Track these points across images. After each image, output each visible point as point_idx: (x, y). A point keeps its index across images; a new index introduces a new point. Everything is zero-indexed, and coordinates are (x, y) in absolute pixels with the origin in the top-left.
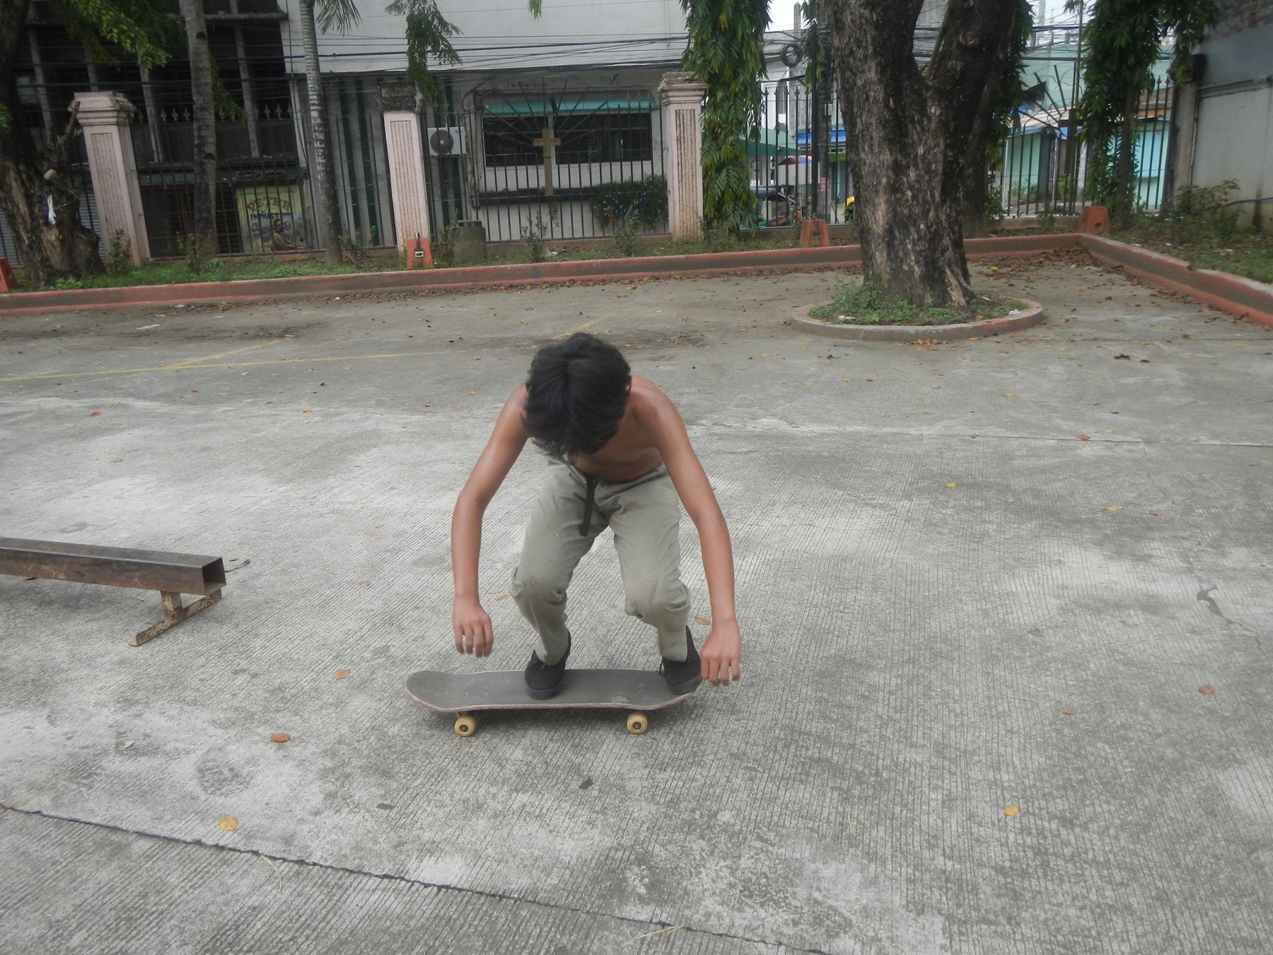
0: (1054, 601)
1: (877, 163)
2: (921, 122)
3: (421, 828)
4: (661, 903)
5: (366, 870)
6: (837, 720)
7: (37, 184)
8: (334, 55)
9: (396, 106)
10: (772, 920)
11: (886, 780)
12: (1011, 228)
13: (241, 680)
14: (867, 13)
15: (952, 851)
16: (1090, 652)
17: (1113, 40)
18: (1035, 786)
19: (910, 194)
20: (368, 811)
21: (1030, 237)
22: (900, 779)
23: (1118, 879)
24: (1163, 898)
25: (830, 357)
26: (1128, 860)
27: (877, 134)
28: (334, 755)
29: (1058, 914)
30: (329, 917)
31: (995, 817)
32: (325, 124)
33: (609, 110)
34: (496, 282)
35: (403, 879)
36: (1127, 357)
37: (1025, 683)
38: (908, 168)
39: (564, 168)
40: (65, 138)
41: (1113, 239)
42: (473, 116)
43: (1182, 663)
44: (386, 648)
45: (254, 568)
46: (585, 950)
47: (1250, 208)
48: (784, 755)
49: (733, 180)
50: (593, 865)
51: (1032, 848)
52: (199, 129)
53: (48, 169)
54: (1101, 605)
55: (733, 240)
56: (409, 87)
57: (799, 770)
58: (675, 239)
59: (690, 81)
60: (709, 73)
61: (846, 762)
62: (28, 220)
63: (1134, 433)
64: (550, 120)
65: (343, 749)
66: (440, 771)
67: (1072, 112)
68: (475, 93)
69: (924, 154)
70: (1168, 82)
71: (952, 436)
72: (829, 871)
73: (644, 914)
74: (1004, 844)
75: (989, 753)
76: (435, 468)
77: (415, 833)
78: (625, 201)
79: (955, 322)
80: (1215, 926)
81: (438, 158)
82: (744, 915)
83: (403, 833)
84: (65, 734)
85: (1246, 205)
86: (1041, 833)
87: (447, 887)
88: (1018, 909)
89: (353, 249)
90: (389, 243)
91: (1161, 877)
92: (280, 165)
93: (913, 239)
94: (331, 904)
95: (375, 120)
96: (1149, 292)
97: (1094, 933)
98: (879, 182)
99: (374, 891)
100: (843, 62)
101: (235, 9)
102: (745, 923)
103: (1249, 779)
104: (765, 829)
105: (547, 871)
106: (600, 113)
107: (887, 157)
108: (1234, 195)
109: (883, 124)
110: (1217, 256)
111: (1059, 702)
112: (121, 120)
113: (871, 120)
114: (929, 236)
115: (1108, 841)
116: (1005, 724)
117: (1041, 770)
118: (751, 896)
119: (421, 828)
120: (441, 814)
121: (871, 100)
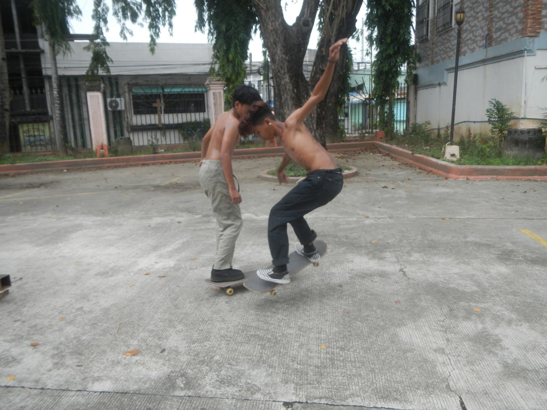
0: (348, 275)
3: (94, 372)
4: (189, 389)
5: (70, 389)
6: (263, 321)
8: (65, 68)
10: (231, 391)
11: (279, 340)
12: (349, 139)
13: (17, 324)
14: (284, 56)
15: (300, 362)
16: (359, 292)
17: (383, 68)
18: (333, 338)
20: (72, 368)
21: (355, 143)
22: (284, 339)
23: (358, 366)
24: (373, 371)
25: (274, 190)
26: (362, 359)
27: (290, 103)
28: (58, 348)
29: (335, 379)
30: (54, 407)
31: (317, 349)
33: (185, 92)
34: (138, 163)
35: (85, 391)
36: (387, 187)
37: (334, 303)
39: (166, 115)
41: (387, 143)
42: (127, 95)
43: (390, 293)
44: (82, 308)
45: (24, 280)
46: (158, 408)
47: (436, 131)
48: (242, 335)
50: (163, 379)
51: (329, 358)
54: (365, 275)
56: (98, 82)
57: (247, 339)
59: (219, 80)
60: (226, 78)
61: (265, 335)
63: (386, 215)
65: (62, 347)
66: (103, 351)
67: (370, 95)
68: (128, 84)
70: (404, 84)
71: (318, 218)
72: (254, 373)
73: (182, 394)
74: (319, 358)
75: (318, 328)
76: (107, 238)
77: (91, 374)
78: (194, 129)
80: (389, 378)
82: (221, 390)
83: (86, 375)
85: (435, 130)
86: (333, 353)
87: (104, 392)
88: (322, 379)
89: (72, 149)
90: (89, 146)
91: (372, 364)
92: (40, 114)
94: (55, 402)
95: (83, 95)
96: (398, 163)
97: (347, 384)
99: (73, 396)
102: (221, 393)
103: (407, 330)
104: (232, 361)
105: (145, 383)
106: (180, 93)
108: (429, 127)
109: (292, 98)
110: (423, 150)
111: (345, 309)
115: (356, 354)
116: (325, 318)
117: (336, 332)
118: (224, 384)
119: (94, 372)
120: (102, 366)
121: (287, 89)
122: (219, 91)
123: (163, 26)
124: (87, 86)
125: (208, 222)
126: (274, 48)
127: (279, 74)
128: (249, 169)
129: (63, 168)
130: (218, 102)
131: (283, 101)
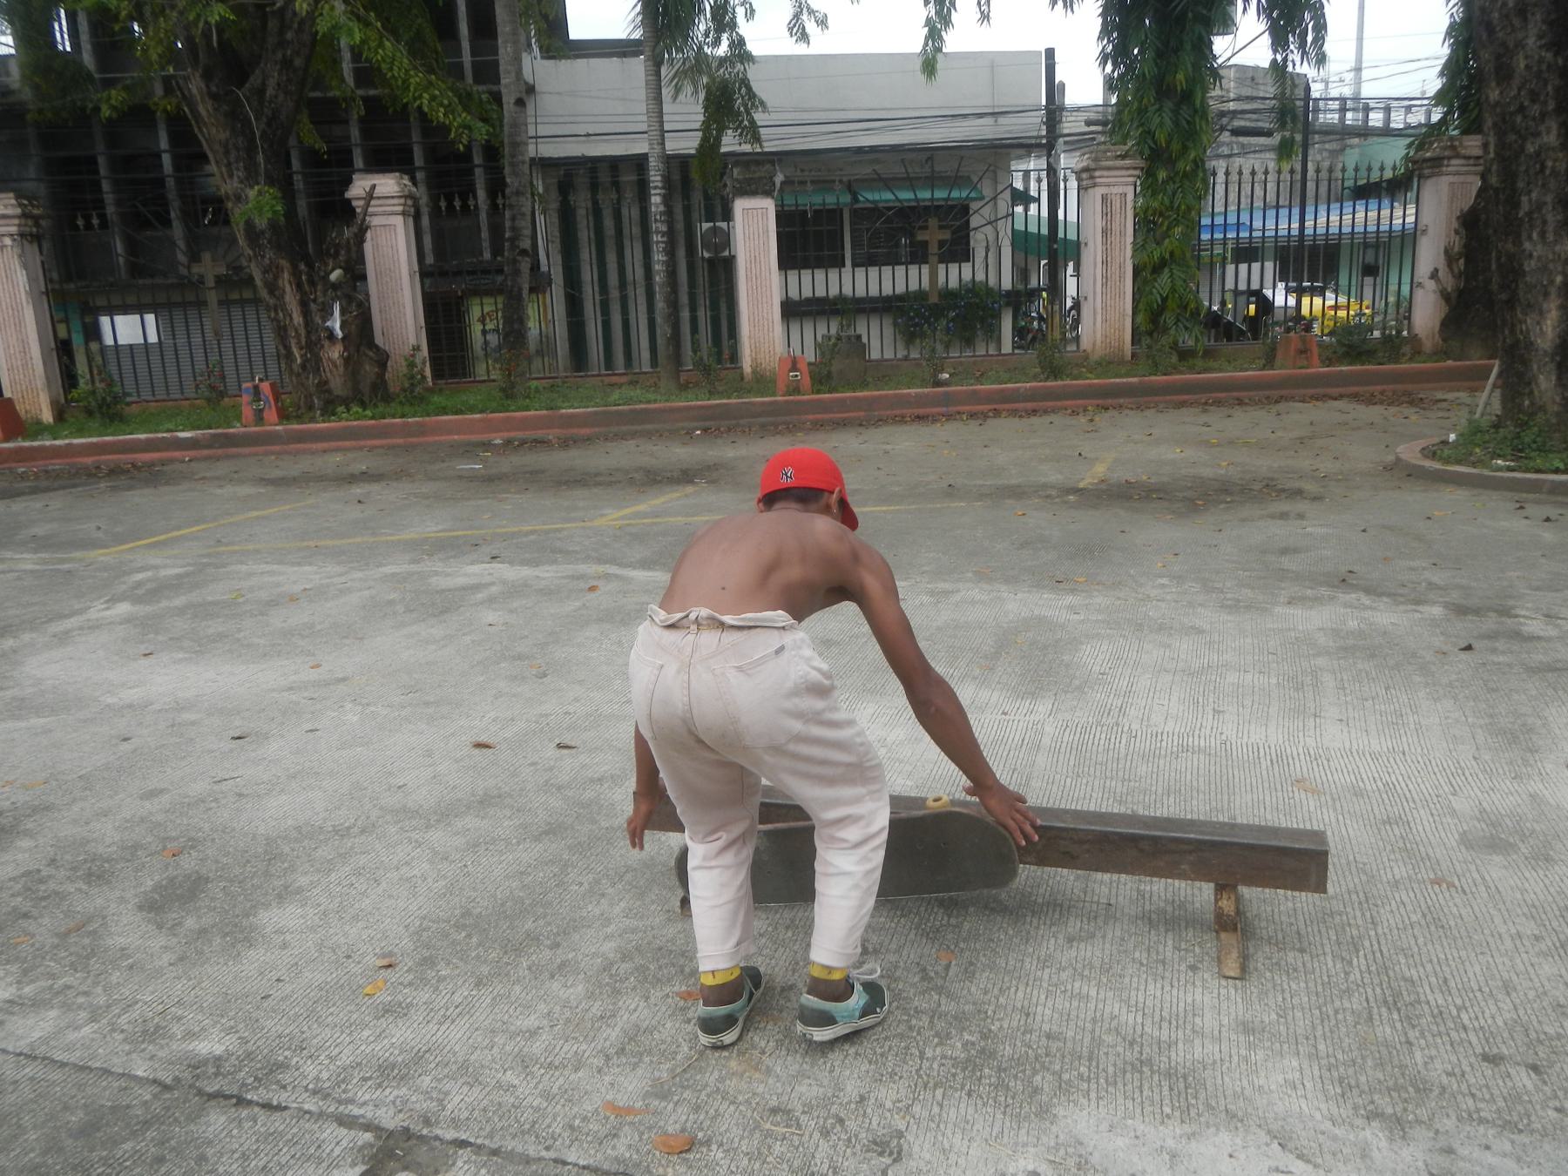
1: (1551, 257)
7: (319, 287)
8: (588, 135)
9: (751, 188)
14: (1549, 56)
25: (1548, 520)
32: (669, 212)
34: (898, 412)
39: (860, 272)
40: (355, 229)
49: (1179, 283)
52: (513, 219)
55: (1174, 359)
56: (768, 166)
58: (1095, 357)
59: (1123, 157)
60: (1150, 147)
62: (303, 332)
76: (1232, 678)
78: (937, 312)
81: (710, 261)
98: (1552, 282)
100: (1504, 119)
101: (469, 79)
121: (1548, 172)
122: (1119, 190)
124: (737, 180)
128: (1301, 440)
129: (686, 424)
130: (1116, 227)
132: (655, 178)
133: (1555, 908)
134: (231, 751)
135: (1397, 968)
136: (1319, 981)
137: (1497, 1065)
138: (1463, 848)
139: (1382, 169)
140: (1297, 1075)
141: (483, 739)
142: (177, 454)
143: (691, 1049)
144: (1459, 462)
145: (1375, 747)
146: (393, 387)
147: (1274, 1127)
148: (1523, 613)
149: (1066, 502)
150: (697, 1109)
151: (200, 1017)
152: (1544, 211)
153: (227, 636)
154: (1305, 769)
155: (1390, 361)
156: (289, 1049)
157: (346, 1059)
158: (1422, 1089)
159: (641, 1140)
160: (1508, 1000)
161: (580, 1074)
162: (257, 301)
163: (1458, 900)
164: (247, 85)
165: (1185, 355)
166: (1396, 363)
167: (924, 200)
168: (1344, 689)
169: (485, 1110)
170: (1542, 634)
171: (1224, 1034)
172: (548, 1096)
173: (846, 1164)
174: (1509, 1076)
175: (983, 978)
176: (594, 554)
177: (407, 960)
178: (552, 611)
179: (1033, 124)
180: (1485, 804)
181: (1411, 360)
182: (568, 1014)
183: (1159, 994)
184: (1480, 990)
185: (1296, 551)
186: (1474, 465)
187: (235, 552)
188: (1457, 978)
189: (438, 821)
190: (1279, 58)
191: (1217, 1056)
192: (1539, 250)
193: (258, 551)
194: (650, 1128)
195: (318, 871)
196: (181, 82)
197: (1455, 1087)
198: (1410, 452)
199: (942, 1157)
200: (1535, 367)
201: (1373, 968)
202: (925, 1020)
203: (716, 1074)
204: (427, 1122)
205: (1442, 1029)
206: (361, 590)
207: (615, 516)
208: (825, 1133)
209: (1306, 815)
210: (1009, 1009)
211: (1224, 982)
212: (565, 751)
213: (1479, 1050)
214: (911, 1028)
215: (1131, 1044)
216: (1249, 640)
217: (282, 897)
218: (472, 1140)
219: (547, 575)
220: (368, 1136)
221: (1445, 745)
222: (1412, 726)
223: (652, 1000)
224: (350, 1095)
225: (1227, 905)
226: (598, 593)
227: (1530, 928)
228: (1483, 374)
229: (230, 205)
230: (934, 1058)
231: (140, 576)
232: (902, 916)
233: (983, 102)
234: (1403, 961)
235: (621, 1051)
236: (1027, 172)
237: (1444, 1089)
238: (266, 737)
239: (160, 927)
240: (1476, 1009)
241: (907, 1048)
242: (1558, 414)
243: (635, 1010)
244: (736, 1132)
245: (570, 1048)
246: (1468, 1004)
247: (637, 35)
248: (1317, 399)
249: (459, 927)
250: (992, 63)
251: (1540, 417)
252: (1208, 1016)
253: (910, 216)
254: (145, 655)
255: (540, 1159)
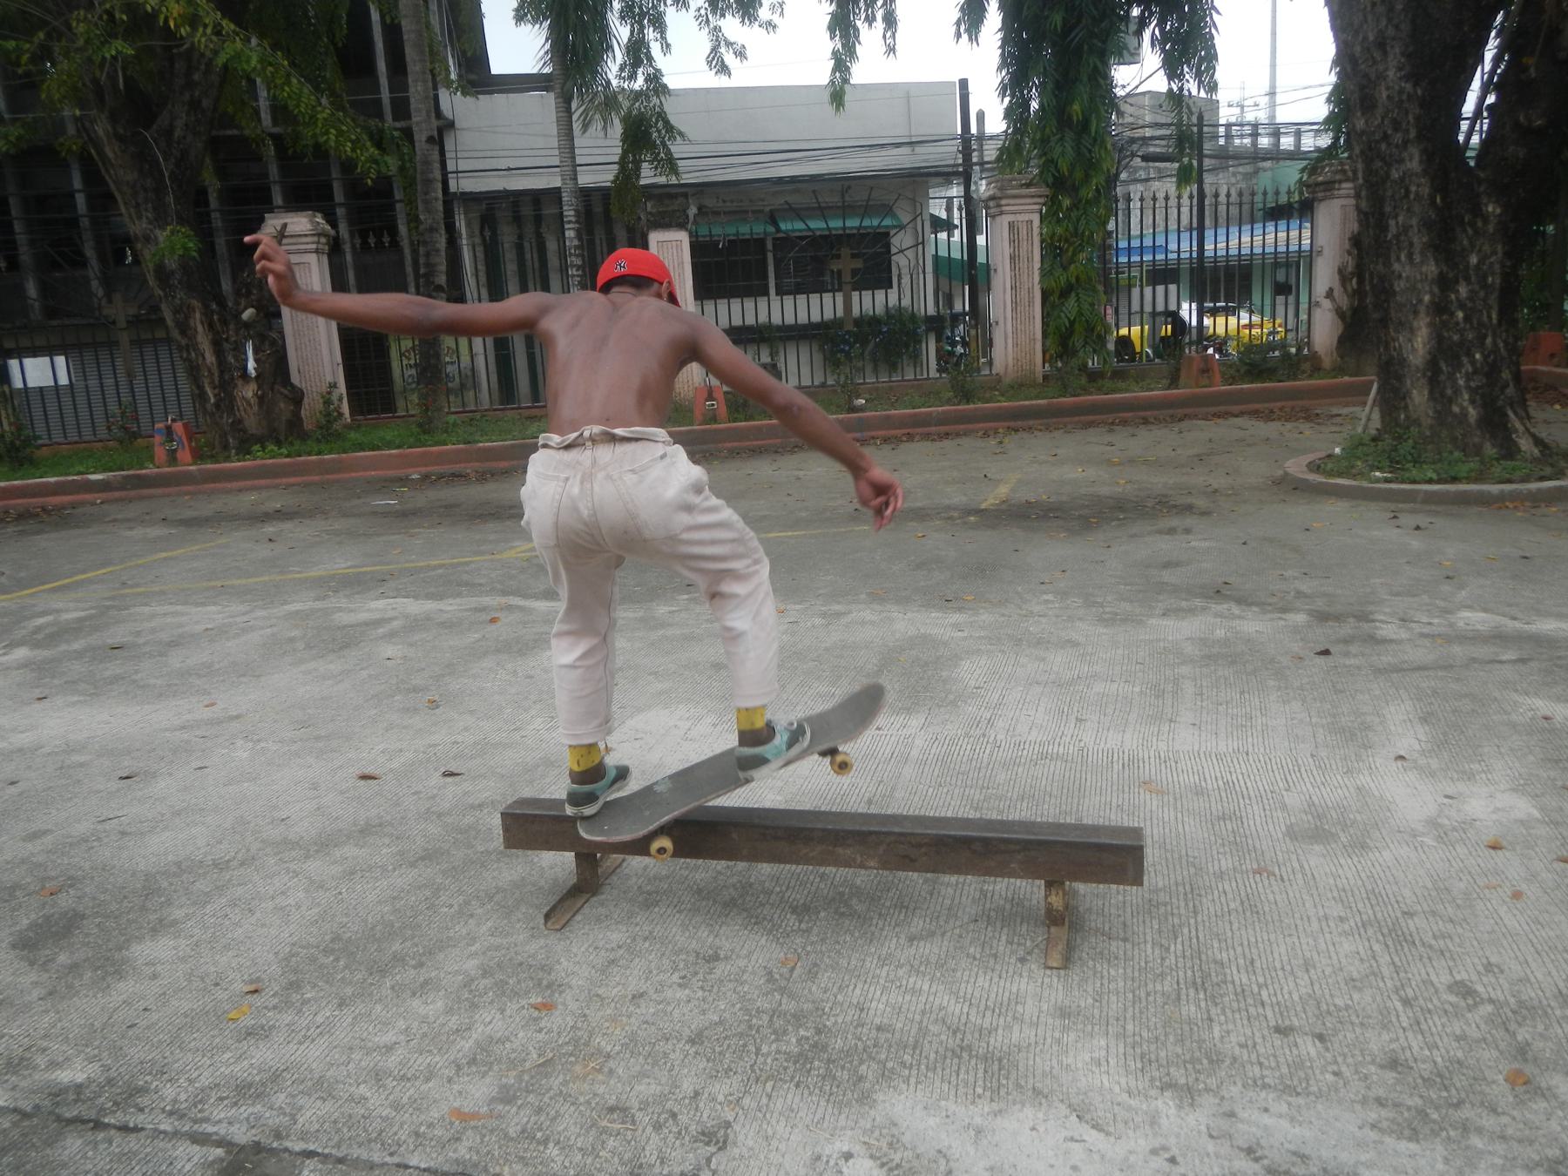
1: (1418, 277)
2: (1473, 225)
7: (232, 326)
8: (509, 169)
14: (1408, 87)
19: (1460, 315)
25: (1418, 528)
27: (1418, 240)
38: (1457, 282)
49: (1086, 306)
52: (428, 255)
53: (246, 309)
55: (1084, 381)
56: (681, 200)
58: (1007, 380)
59: (1028, 185)
64: (769, 246)
69: (1479, 262)
76: (1099, 687)
79: (1542, 479)
84: (1154, 1152)
93: (1467, 373)
98: (1420, 301)
100: (1370, 149)
107: (1431, 269)
112: (320, 246)
113: (1407, 223)
114: (1486, 369)
121: (1412, 196)
122: (1026, 217)
123: (866, 25)
125: (1373, 640)
126: (1375, 62)
127: (1383, 146)
130: (1023, 253)
131: (1390, 236)
132: (569, 213)
133: (1363, 891)
134: (118, 790)
135: (1210, 953)
136: (1137, 967)
137: (1286, 1035)
138: (1287, 839)
139: (1277, 193)
140: (1103, 1053)
141: (369, 771)
142: (88, 497)
143: (540, 1056)
144: (1340, 475)
145: (1222, 748)
146: (308, 425)
147: (1074, 1101)
148: (1382, 617)
149: (965, 523)
150: (539, 1111)
151: (64, 1048)
152: (1410, 234)
153: (123, 678)
154: (1153, 770)
155: (1289, 379)
156: (150, 1074)
157: (205, 1080)
158: (1215, 1059)
159: (482, 1142)
160: (1306, 977)
161: (430, 1084)
162: (168, 340)
163: (1275, 888)
164: (155, 127)
165: (1094, 376)
166: (1295, 379)
167: (836, 229)
168: (1202, 694)
169: (335, 1122)
170: (1394, 637)
171: (1042, 1019)
172: (397, 1106)
173: (673, 1154)
174: (1296, 1045)
175: (825, 978)
176: (499, 586)
177: (273, 984)
178: (451, 643)
179: (948, 153)
180: (1314, 798)
181: (1310, 377)
182: (425, 1029)
183: (987, 985)
184: (1283, 969)
185: (1177, 564)
186: (1354, 477)
187: (139, 594)
188: (1263, 958)
189: (317, 851)
190: (1175, 89)
191: (1033, 1039)
192: (1407, 271)
193: (163, 593)
194: (492, 1131)
195: (195, 903)
196: (87, 124)
197: (1245, 1058)
198: (1296, 466)
199: (765, 1144)
200: (1409, 382)
201: (1188, 954)
202: (766, 1018)
203: (561, 1076)
204: (278, 1136)
205: (1242, 1005)
206: (262, 628)
207: (523, 548)
208: (658, 1127)
209: (1148, 815)
210: (845, 1006)
211: (1048, 972)
212: (449, 779)
213: (1273, 1023)
214: (750, 1027)
215: (955, 1033)
216: (1120, 652)
217: (154, 930)
218: (320, 1151)
219: (450, 608)
220: (220, 1152)
221: (1287, 744)
222: (1259, 728)
223: (508, 1012)
224: (206, 1114)
225: (1056, 901)
226: (499, 624)
227: (1336, 910)
228: (1364, 388)
229: (139, 246)
230: (769, 1054)
231: (40, 621)
232: (756, 923)
233: (899, 132)
234: (1216, 945)
235: (473, 1061)
236: (942, 201)
237: (1235, 1059)
238: (154, 775)
239: (32, 964)
240: (1276, 986)
241: (745, 1045)
242: (1431, 427)
243: (490, 1023)
244: (574, 1130)
245: (422, 1062)
246: (1269, 982)
247: (547, 70)
248: (1219, 417)
249: (327, 951)
250: (906, 95)
251: (1414, 430)
252: (1029, 1002)
253: (829, 243)
254: (40, 699)
255: (384, 1164)
